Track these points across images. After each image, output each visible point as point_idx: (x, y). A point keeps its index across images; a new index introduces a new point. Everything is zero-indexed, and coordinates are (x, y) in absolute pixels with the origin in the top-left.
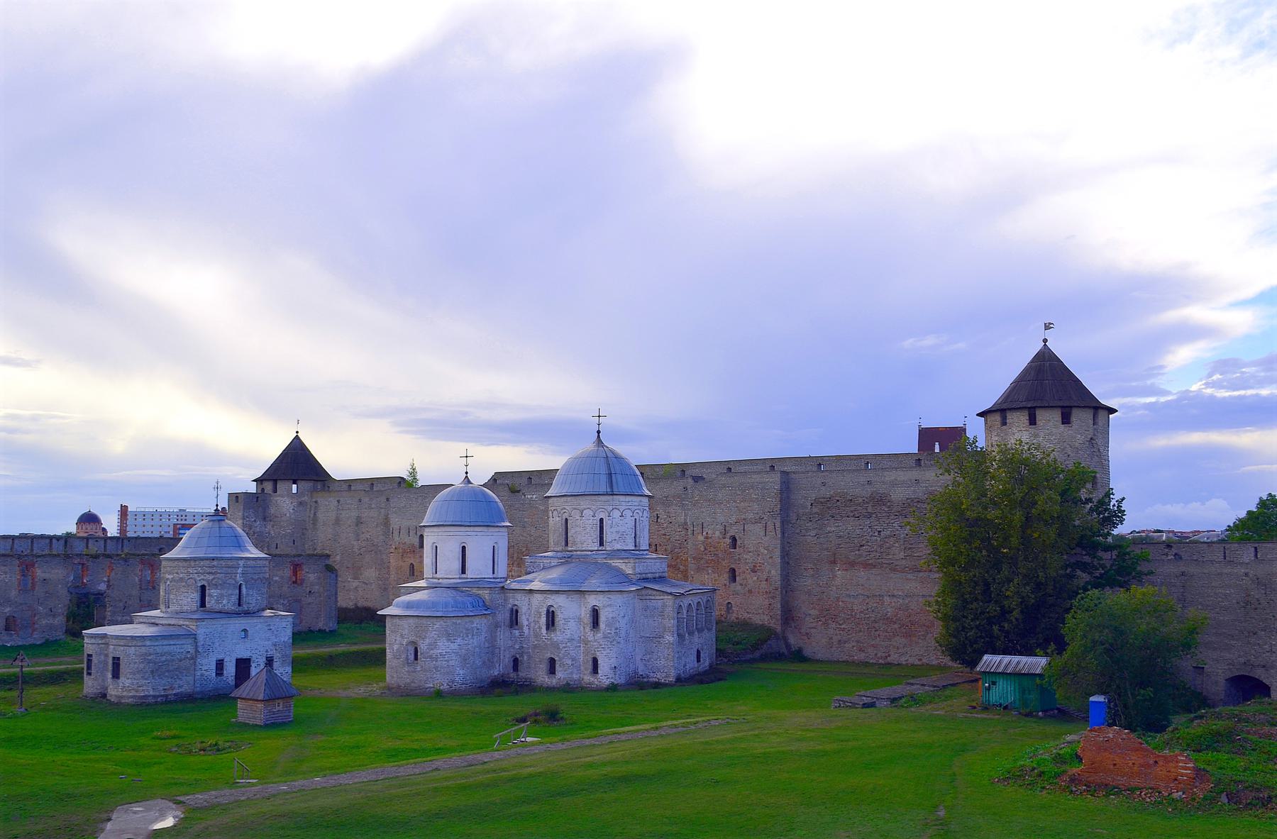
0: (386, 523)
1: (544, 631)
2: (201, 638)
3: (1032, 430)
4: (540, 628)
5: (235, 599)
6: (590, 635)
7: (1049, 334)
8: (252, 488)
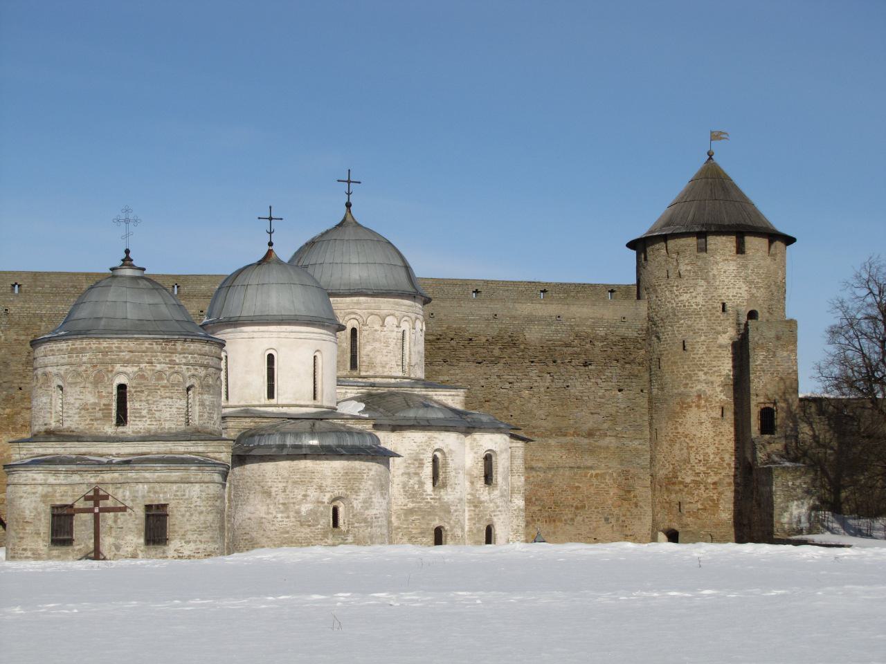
1: (429, 486)
3: (740, 259)
4: (421, 484)
6: (484, 493)
7: (717, 147)
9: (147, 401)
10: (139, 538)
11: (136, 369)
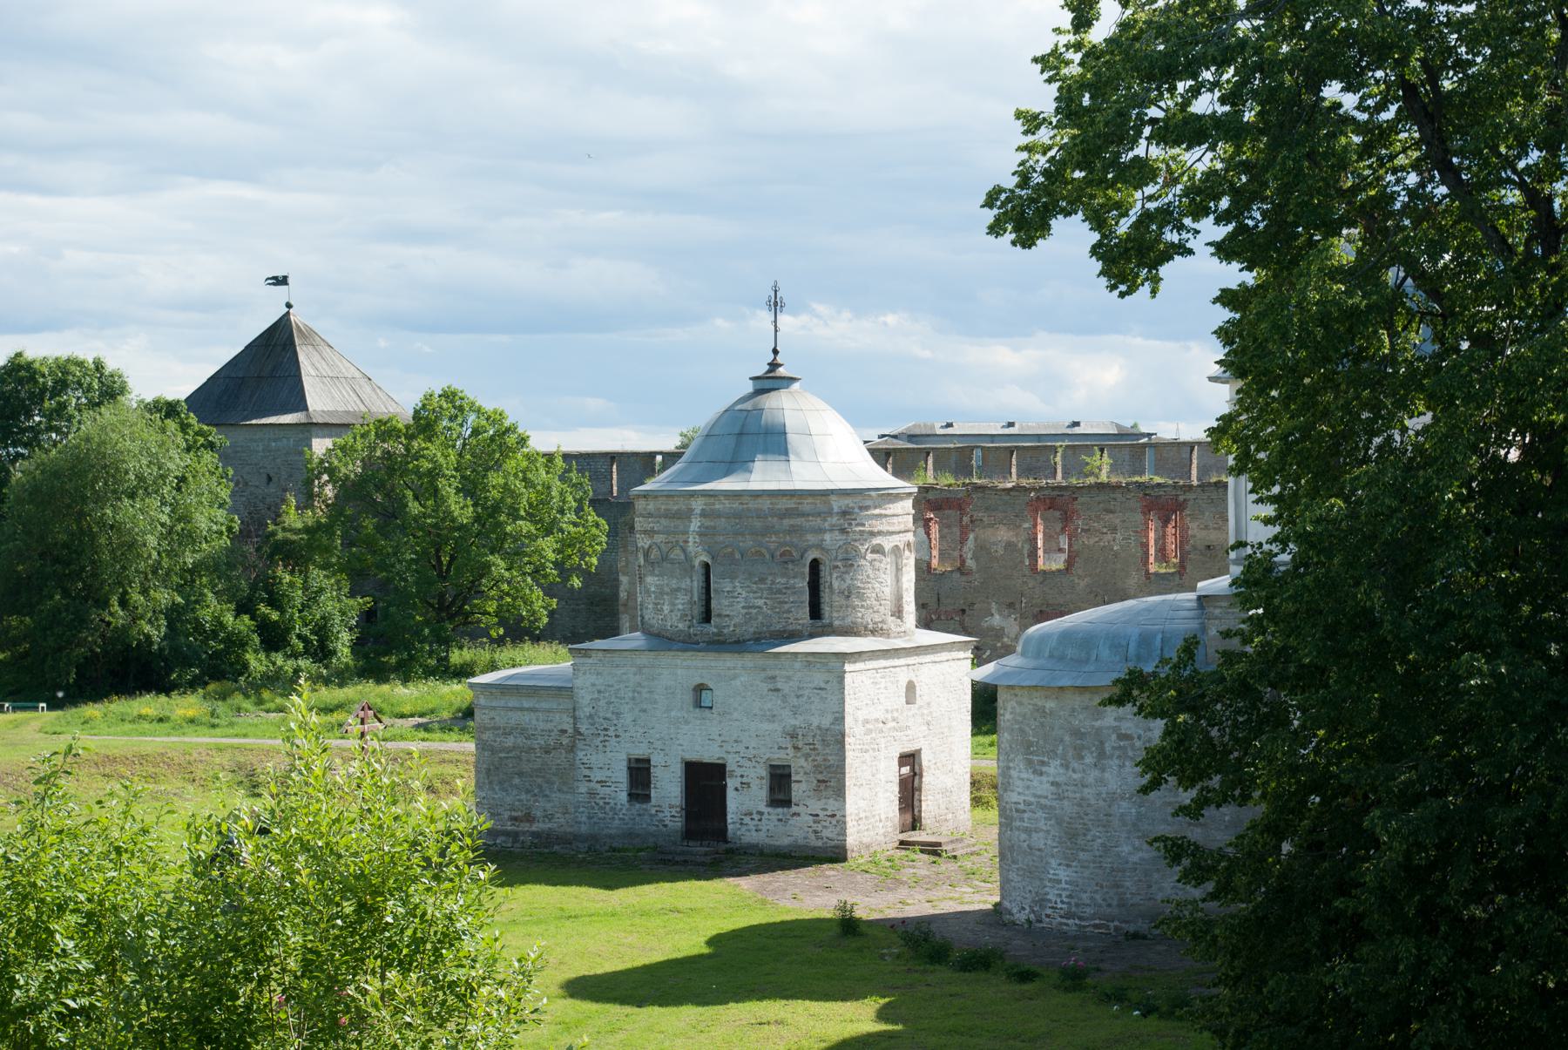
2: (585, 698)
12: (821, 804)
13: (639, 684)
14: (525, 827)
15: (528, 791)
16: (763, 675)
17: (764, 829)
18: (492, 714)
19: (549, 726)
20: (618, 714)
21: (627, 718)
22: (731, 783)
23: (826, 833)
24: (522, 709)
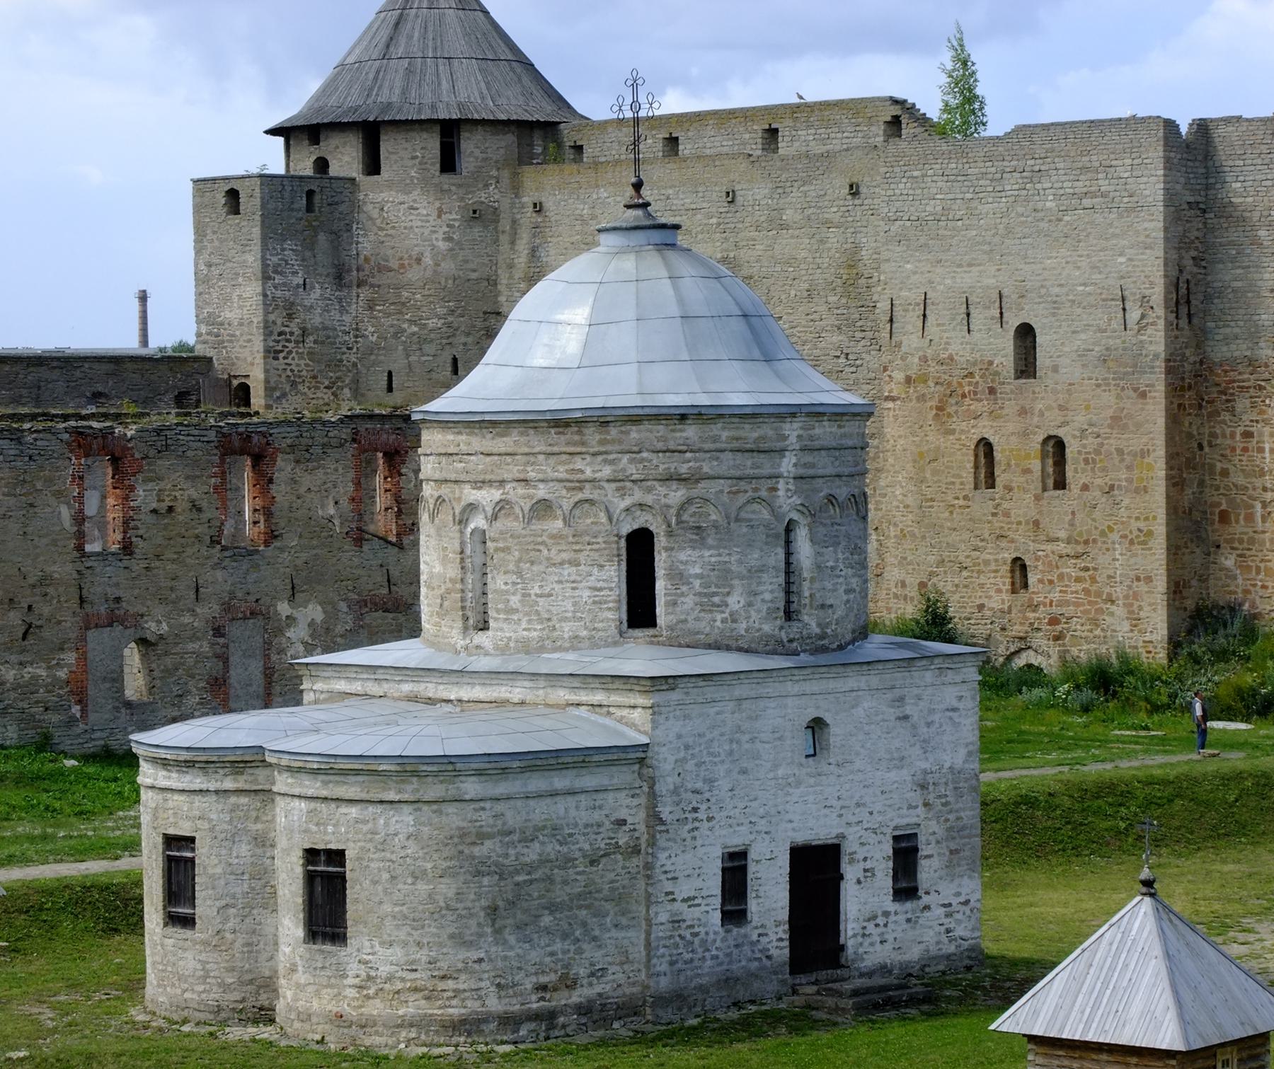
0: (854, 279)
2: (665, 760)
5: (771, 587)
8: (272, 157)
9: (519, 573)
10: (297, 927)
11: (497, 494)
12: (953, 888)
13: (739, 729)
14: (562, 999)
15: (565, 936)
16: (889, 696)
17: (890, 937)
18: (500, 807)
19: (597, 816)
20: (710, 781)
21: (724, 784)
22: (850, 872)
23: (960, 932)
24: (554, 794)
